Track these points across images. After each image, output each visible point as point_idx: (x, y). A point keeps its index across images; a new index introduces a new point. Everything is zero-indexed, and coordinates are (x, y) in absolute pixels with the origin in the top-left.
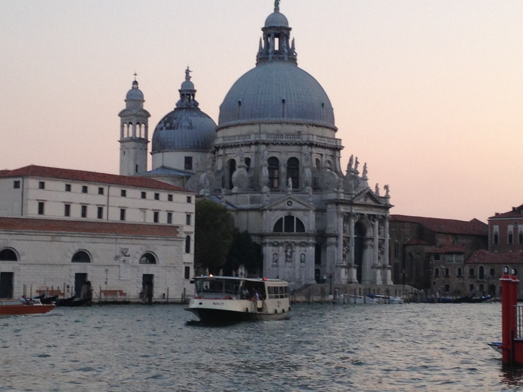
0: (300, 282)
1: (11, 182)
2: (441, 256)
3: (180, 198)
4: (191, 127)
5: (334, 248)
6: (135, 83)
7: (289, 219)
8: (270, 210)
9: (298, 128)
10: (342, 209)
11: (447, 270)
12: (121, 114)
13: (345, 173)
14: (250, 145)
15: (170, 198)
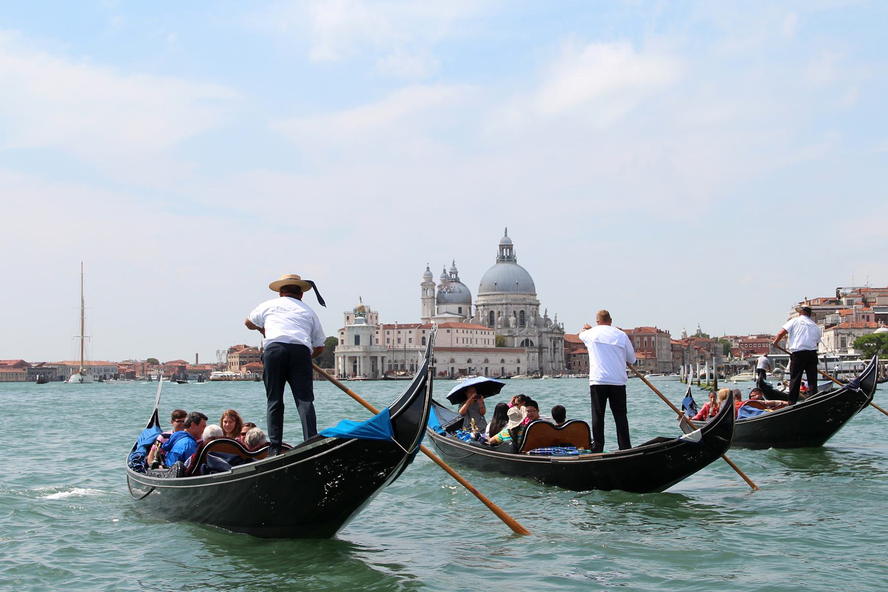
0: (532, 369)
1: (446, 330)
2: (576, 355)
3: (491, 333)
4: (460, 292)
5: (546, 353)
6: (428, 268)
7: (527, 340)
8: (519, 336)
9: (524, 296)
10: (550, 336)
11: (579, 362)
12: (422, 284)
13: (542, 316)
14: (503, 304)
15: (488, 334)
